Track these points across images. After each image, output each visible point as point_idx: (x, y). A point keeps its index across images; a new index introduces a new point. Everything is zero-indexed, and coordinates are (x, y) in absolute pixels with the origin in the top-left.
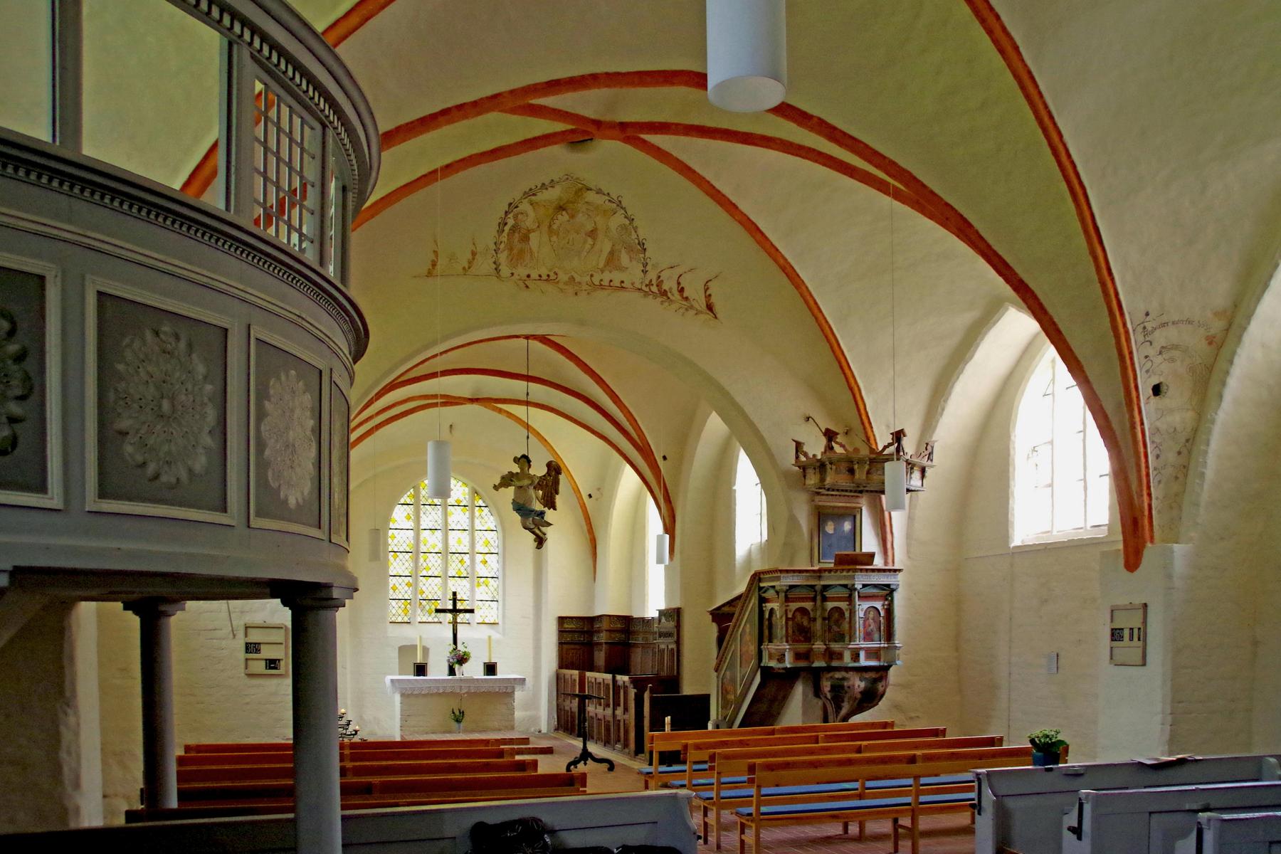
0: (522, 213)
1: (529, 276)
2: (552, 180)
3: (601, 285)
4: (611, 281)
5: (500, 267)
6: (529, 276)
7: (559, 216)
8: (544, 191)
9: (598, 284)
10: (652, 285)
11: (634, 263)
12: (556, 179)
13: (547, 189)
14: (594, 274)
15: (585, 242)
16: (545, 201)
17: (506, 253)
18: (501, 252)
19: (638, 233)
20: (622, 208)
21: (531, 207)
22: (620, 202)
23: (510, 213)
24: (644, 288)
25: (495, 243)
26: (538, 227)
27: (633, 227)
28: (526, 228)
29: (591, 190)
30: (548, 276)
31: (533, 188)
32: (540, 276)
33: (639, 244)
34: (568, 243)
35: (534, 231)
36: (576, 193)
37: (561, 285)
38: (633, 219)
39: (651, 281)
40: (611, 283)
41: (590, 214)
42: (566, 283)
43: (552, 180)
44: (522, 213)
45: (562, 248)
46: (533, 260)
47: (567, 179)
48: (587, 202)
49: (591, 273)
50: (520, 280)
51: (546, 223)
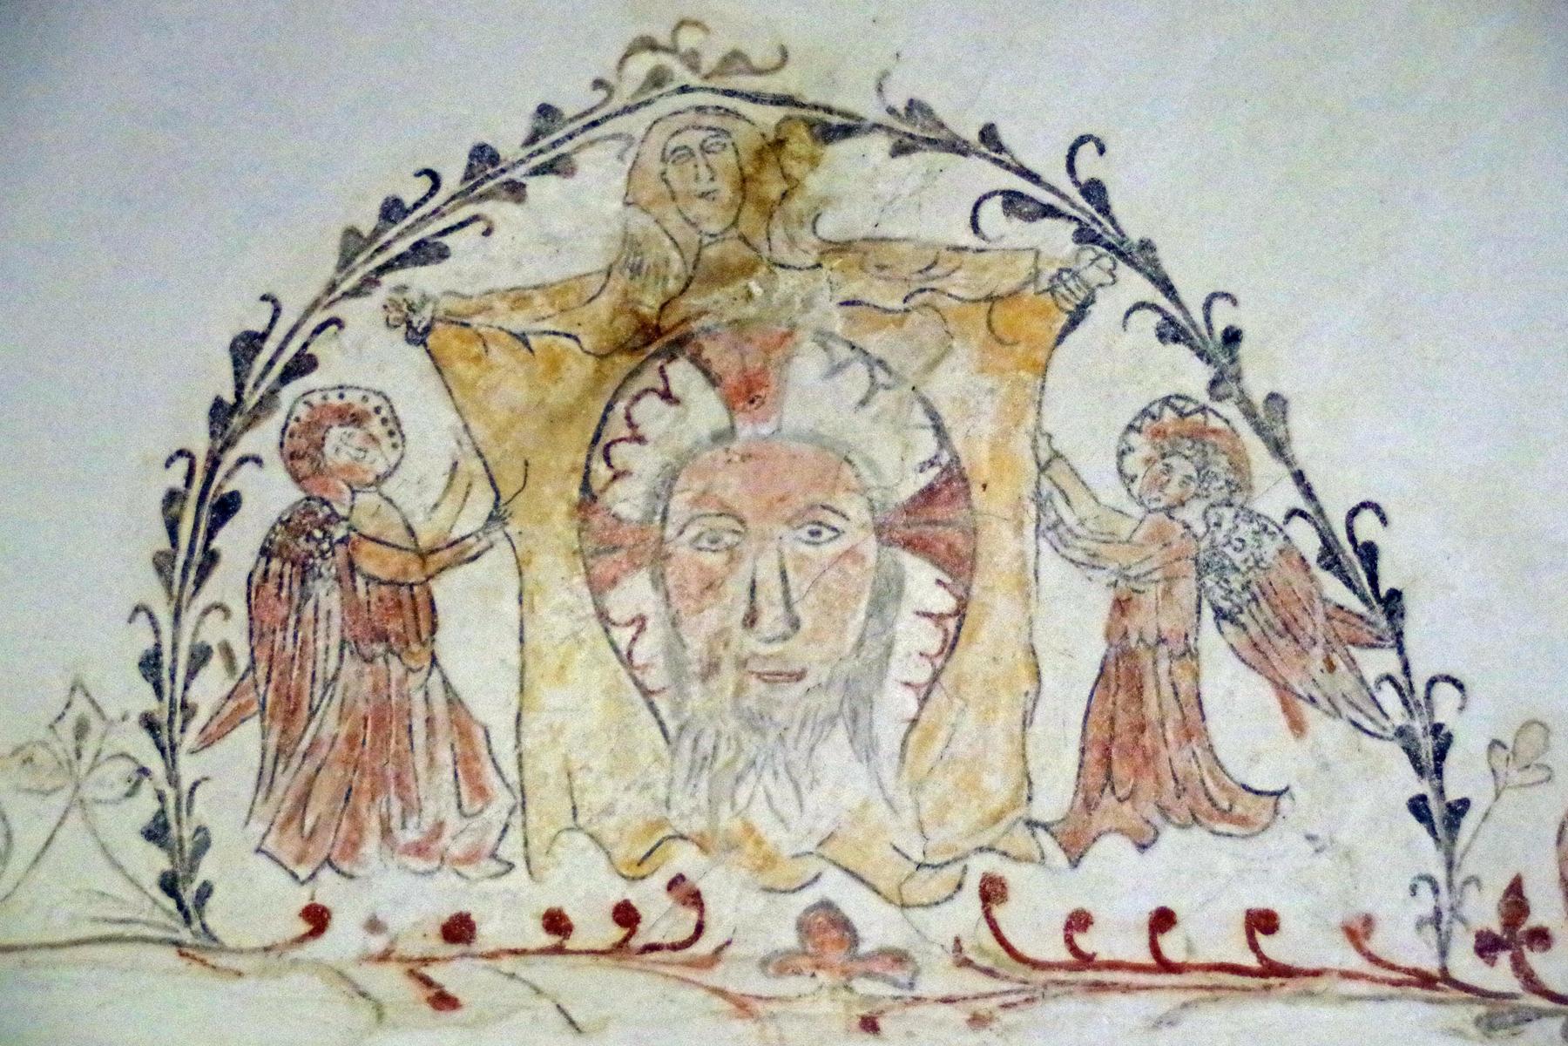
0: (356, 419)
1: (458, 930)
2: (546, 111)
3: (1085, 961)
4: (1163, 920)
5: (207, 869)
6: (458, 930)
7: (650, 412)
8: (486, 208)
9: (1065, 956)
10: (1541, 937)
11: (1327, 731)
12: (573, 98)
13: (516, 191)
14: (1010, 872)
15: (887, 595)
16: (519, 298)
17: (248, 740)
18: (208, 740)
19: (1300, 450)
20: (1120, 252)
21: (417, 353)
22: (1094, 191)
23: (253, 420)
24: (1466, 965)
25: (150, 664)
26: (496, 517)
27: (1250, 413)
28: (397, 535)
29: (849, 129)
30: (626, 915)
31: (414, 191)
32: (556, 922)
33: (1330, 558)
34: (751, 620)
35: (460, 552)
36: (744, 182)
37: (741, 978)
38: (1232, 337)
39: (1515, 900)
40: (1172, 946)
41: (875, 343)
42: (778, 964)
43: (546, 111)
44: (356, 419)
45: (711, 669)
46: (481, 791)
47: (657, 79)
48: (840, 248)
49: (981, 866)
50: (384, 957)
51: (559, 494)
